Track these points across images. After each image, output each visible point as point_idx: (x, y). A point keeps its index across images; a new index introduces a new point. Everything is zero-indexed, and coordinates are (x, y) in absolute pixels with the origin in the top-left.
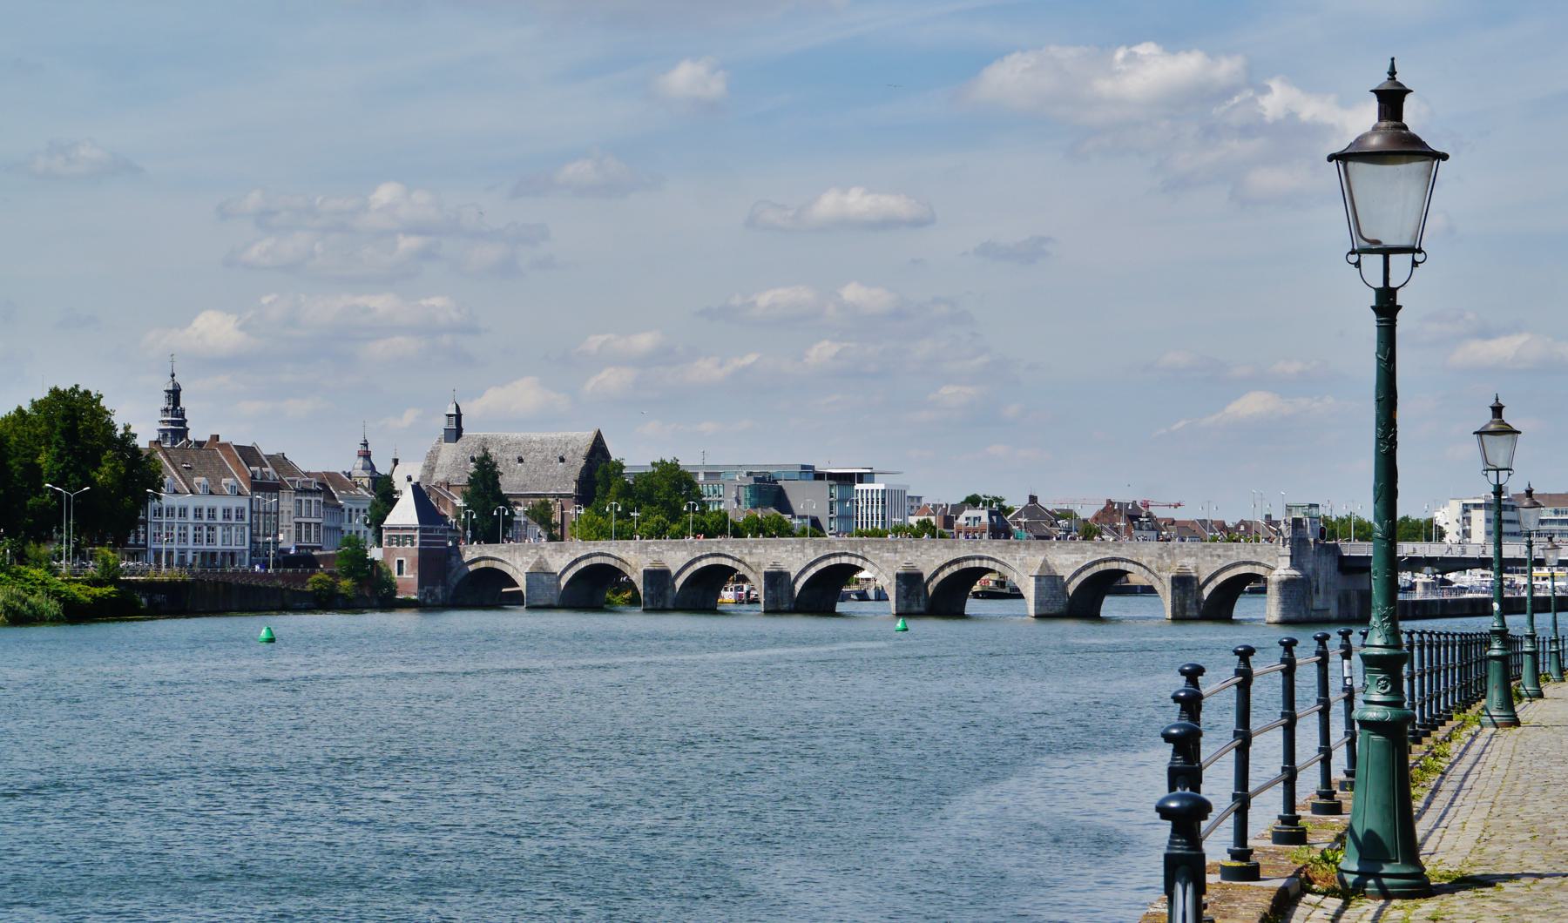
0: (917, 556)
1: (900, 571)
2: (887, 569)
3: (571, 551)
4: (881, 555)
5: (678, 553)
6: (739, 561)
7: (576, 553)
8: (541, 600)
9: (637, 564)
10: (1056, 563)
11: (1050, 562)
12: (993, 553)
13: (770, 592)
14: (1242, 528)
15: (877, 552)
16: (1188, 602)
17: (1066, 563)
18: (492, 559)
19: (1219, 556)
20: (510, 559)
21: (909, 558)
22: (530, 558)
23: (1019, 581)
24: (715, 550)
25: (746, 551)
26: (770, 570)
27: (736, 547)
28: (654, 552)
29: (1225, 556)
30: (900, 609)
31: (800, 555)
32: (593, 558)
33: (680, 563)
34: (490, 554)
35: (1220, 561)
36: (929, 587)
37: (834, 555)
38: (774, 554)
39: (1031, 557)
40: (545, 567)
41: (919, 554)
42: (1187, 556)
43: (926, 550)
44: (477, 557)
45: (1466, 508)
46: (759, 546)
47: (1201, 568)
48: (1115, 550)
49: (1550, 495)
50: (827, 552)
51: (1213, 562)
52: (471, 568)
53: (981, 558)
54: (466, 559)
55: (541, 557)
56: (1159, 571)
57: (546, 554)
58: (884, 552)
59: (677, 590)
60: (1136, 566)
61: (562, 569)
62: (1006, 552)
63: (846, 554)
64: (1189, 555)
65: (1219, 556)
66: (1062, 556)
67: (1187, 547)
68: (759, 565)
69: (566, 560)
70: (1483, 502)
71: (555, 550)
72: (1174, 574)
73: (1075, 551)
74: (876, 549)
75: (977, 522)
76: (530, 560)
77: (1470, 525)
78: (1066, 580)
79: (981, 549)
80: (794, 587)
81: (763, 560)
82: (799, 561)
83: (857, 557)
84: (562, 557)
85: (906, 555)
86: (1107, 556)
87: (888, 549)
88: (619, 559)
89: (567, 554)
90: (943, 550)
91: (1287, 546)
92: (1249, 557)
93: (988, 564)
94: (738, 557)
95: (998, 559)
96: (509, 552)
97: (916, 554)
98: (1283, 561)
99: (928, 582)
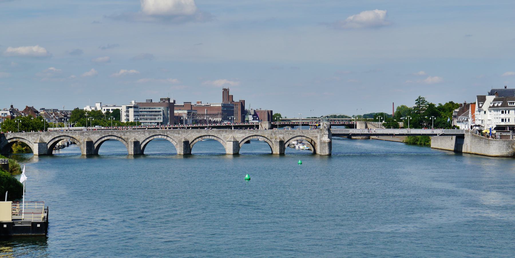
0: (187, 135)
1: (183, 140)
2: (176, 140)
3: (52, 135)
4: (173, 135)
5: (96, 135)
6: (120, 138)
7: (54, 136)
8: (42, 152)
9: (79, 139)
10: (236, 137)
11: (234, 137)
12: (214, 134)
13: (135, 148)
16: (282, 148)
17: (239, 137)
18: (19, 138)
19: (291, 134)
20: (27, 138)
21: (184, 136)
22: (35, 137)
23: (222, 143)
24: (110, 134)
25: (123, 134)
26: (135, 141)
27: (120, 133)
28: (86, 135)
29: (293, 134)
30: (184, 153)
31: (143, 135)
32: (61, 137)
34: (18, 136)
35: (291, 136)
36: (191, 145)
37: (156, 135)
39: (227, 135)
40: (43, 140)
42: (280, 134)
44: (12, 137)
45: (128, 108)
47: (285, 138)
48: (256, 133)
49: (143, 103)
50: (153, 134)
51: (289, 136)
52: (9, 141)
53: (209, 136)
54: (7, 138)
55: (40, 137)
56: (271, 139)
57: (42, 136)
58: (174, 134)
59: (95, 148)
60: (263, 138)
61: (48, 141)
62: (219, 134)
64: (281, 134)
65: (291, 134)
66: (238, 135)
67: (281, 131)
68: (128, 139)
69: (50, 138)
70: (133, 106)
71: (46, 135)
72: (279, 140)
73: (243, 133)
74: (172, 133)
75: (6, 115)
76: (35, 138)
77: (128, 113)
78: (239, 142)
79: (209, 132)
80: (141, 146)
81: (129, 137)
82: (143, 137)
83: (165, 135)
84: (48, 137)
85: (182, 135)
86: (253, 134)
88: (72, 137)
89: (51, 136)
90: (196, 133)
91: (327, 131)
92: (300, 134)
93: (212, 137)
94: (119, 136)
95: (216, 136)
96: (26, 135)
98: (326, 136)
99: (191, 144)
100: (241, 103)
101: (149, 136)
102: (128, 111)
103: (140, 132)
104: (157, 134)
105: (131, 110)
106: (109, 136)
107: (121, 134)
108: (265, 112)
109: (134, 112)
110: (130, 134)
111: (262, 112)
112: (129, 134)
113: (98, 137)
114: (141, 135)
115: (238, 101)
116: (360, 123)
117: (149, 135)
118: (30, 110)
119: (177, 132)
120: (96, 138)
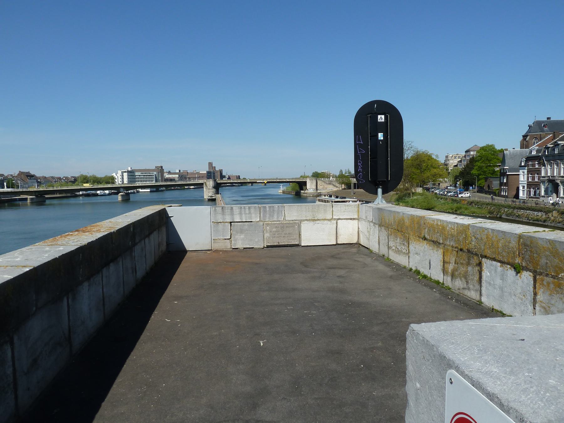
14: (64, 178)
45: (122, 173)
100: (220, 171)
102: (123, 176)
105: (125, 175)
108: (235, 176)
109: (128, 175)
111: (233, 176)
115: (218, 170)
116: (310, 180)
118: (23, 174)
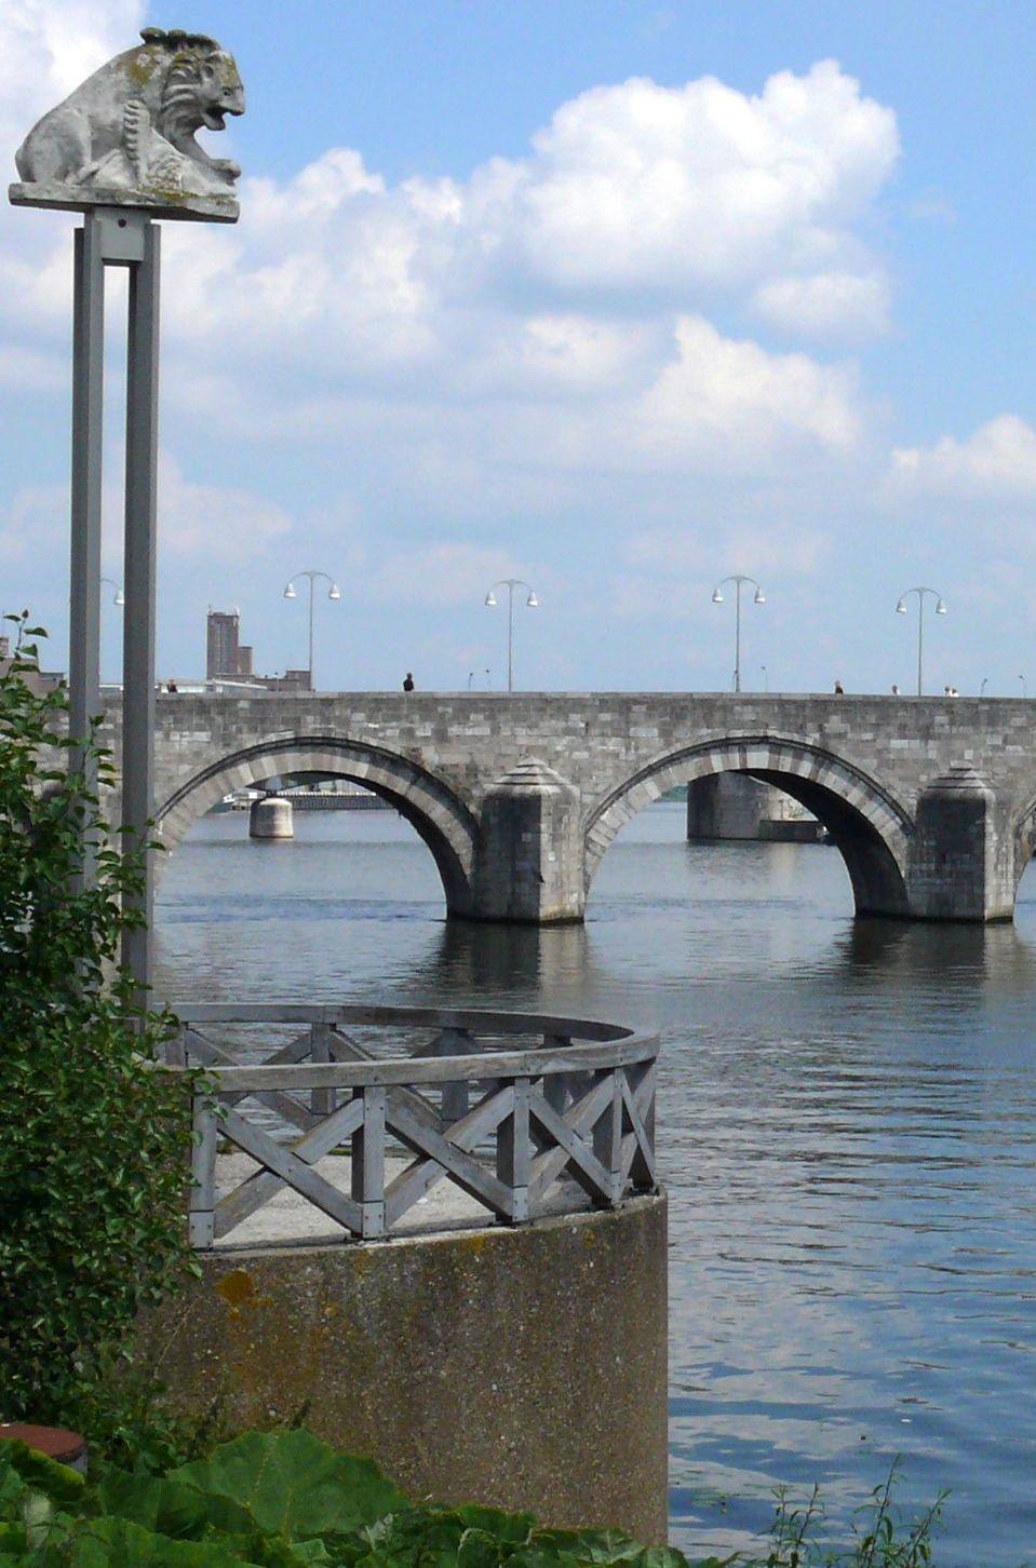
0: (995, 748)
4: (879, 744)
5: (175, 737)
15: (868, 736)
24: (311, 726)
27: (398, 718)
31: (613, 744)
33: (185, 768)
37: (724, 745)
38: (522, 741)
41: (999, 741)
43: (1021, 729)
46: (472, 716)
50: (705, 734)
58: (889, 736)
63: (765, 740)
81: (484, 760)
82: (610, 763)
83: (800, 750)
85: (957, 744)
87: (903, 727)
94: (396, 748)
97: (989, 743)
101: (666, 753)
103: (588, 715)
104: (739, 733)
106: (300, 743)
107: (409, 733)
110: (495, 730)
112: (486, 731)
113: (197, 754)
114: (594, 743)
117: (668, 744)
119: (911, 722)
120: (181, 758)
